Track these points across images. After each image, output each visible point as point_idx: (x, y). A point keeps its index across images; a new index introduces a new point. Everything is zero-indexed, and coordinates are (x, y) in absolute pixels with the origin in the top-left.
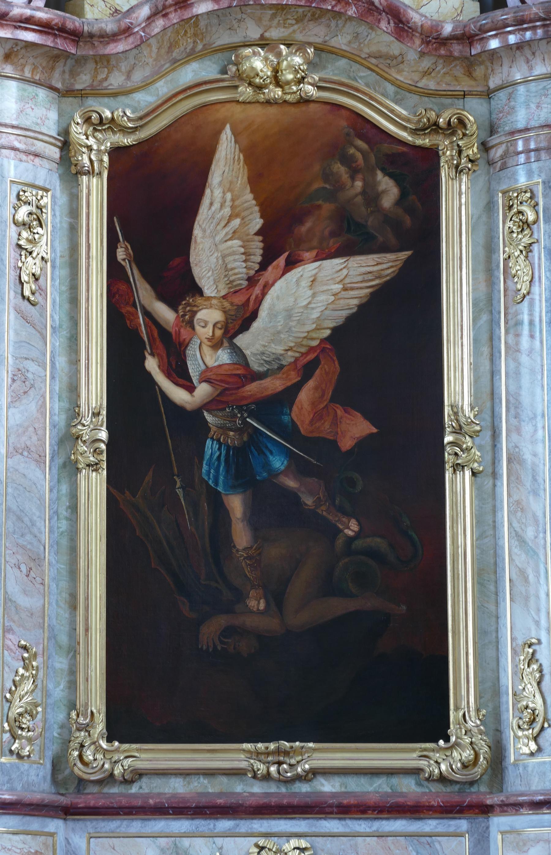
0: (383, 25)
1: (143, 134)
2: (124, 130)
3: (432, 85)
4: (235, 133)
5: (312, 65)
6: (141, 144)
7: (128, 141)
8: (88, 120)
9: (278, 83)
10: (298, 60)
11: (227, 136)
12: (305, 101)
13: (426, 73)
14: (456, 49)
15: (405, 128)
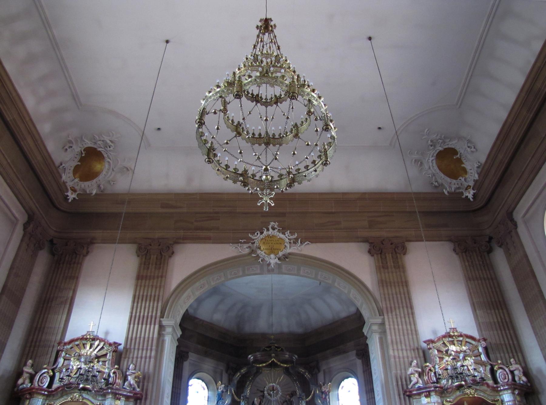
0: (485, 385)
1: (454, 402)
2: (451, 402)
3: (491, 394)
4: (466, 401)
5: (475, 392)
6: (454, 404)
7: (452, 404)
8: (446, 401)
9: (471, 394)
10: (473, 391)
11: (465, 402)
12: (470, 397)
13: (491, 392)
14: (496, 389)
15: (490, 401)
